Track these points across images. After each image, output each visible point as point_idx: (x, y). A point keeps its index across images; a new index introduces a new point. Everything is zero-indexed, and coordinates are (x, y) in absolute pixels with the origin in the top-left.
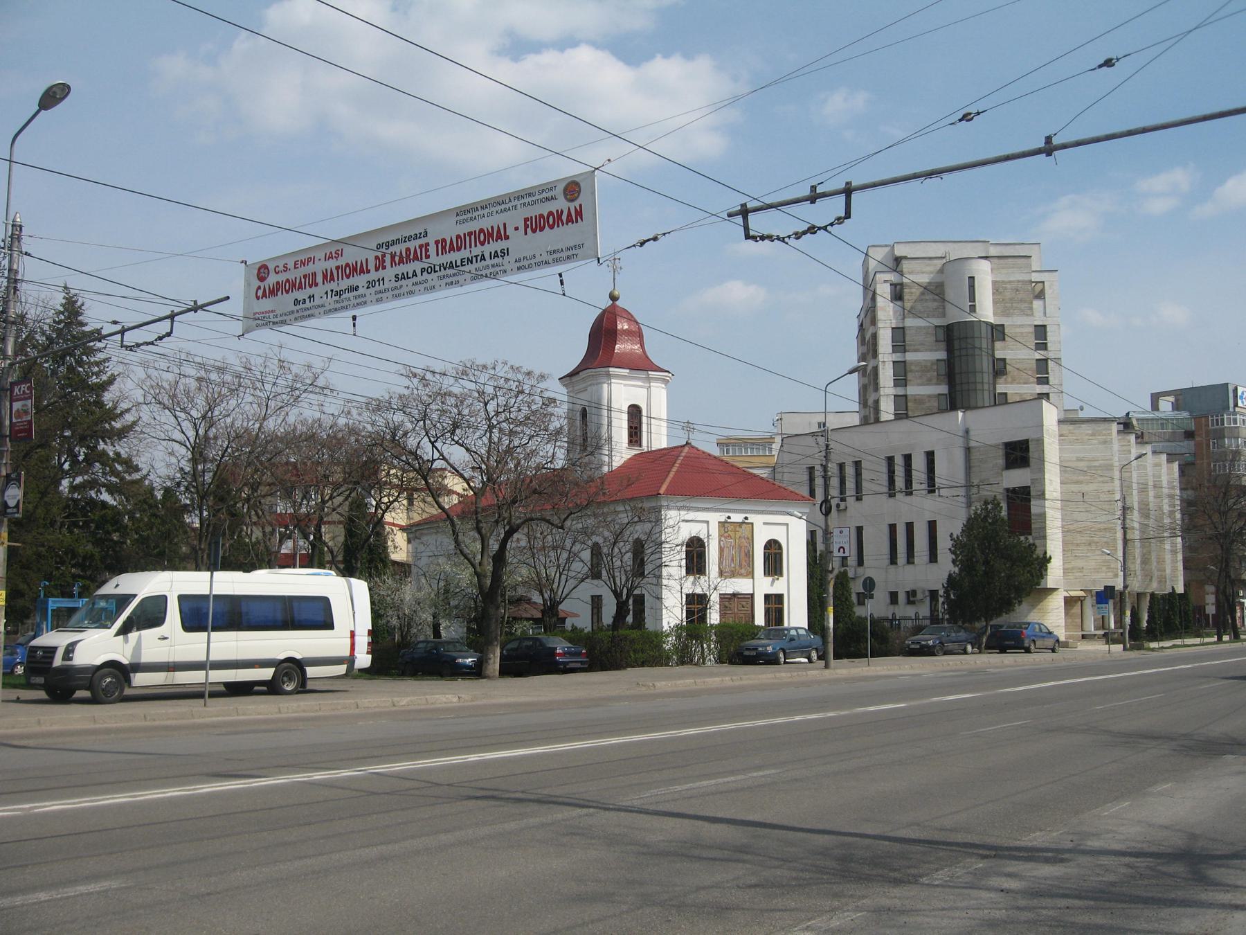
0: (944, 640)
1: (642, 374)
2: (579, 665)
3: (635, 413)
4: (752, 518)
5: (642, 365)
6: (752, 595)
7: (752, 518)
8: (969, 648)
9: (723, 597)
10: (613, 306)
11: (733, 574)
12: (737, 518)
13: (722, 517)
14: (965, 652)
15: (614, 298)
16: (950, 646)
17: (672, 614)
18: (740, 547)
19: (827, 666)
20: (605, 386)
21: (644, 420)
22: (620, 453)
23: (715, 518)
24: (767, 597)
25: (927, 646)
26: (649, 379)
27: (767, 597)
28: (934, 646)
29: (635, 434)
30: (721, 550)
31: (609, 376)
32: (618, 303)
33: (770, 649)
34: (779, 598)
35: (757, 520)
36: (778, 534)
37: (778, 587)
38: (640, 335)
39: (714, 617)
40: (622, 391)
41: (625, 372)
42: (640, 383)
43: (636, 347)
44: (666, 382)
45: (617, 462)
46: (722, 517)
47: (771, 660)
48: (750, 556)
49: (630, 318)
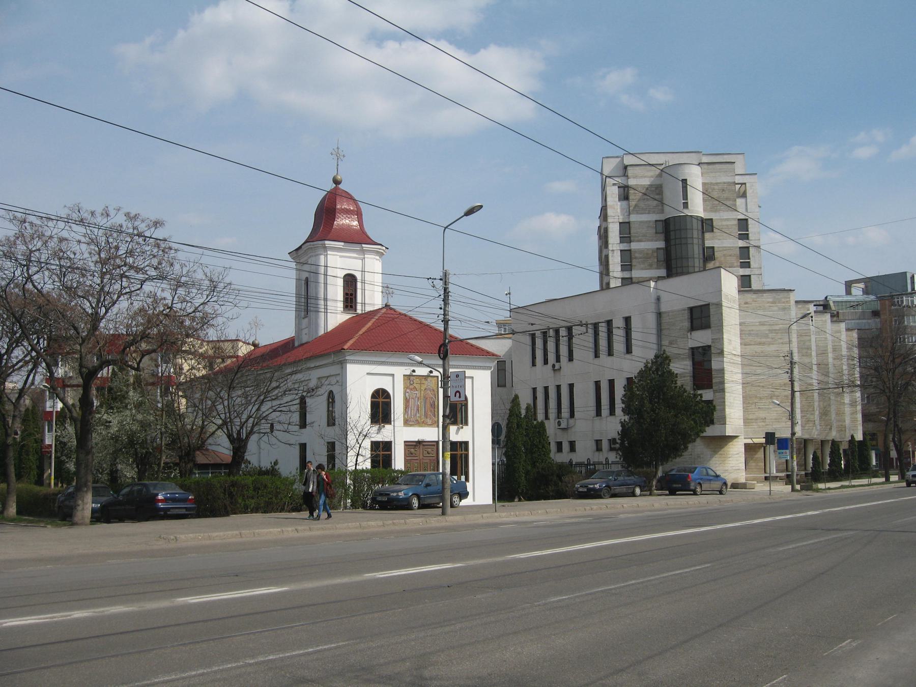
0: (611, 483)
2: (183, 511)
3: (350, 281)
5: (358, 239)
8: (638, 491)
9: (408, 444)
10: (336, 189)
11: (418, 423)
13: (407, 371)
14: (633, 495)
15: (337, 182)
16: (618, 490)
17: (358, 459)
18: (425, 398)
19: (443, 514)
20: (322, 257)
21: (359, 285)
22: (335, 316)
23: (400, 372)
25: (594, 489)
26: (363, 252)
28: (600, 490)
29: (350, 301)
30: (407, 401)
31: (325, 248)
32: (340, 186)
33: (401, 495)
38: (359, 214)
39: (399, 462)
40: (337, 262)
41: (340, 244)
42: (355, 255)
43: (355, 223)
44: (381, 255)
45: (331, 326)
46: (407, 371)
47: (404, 505)
49: (350, 198)
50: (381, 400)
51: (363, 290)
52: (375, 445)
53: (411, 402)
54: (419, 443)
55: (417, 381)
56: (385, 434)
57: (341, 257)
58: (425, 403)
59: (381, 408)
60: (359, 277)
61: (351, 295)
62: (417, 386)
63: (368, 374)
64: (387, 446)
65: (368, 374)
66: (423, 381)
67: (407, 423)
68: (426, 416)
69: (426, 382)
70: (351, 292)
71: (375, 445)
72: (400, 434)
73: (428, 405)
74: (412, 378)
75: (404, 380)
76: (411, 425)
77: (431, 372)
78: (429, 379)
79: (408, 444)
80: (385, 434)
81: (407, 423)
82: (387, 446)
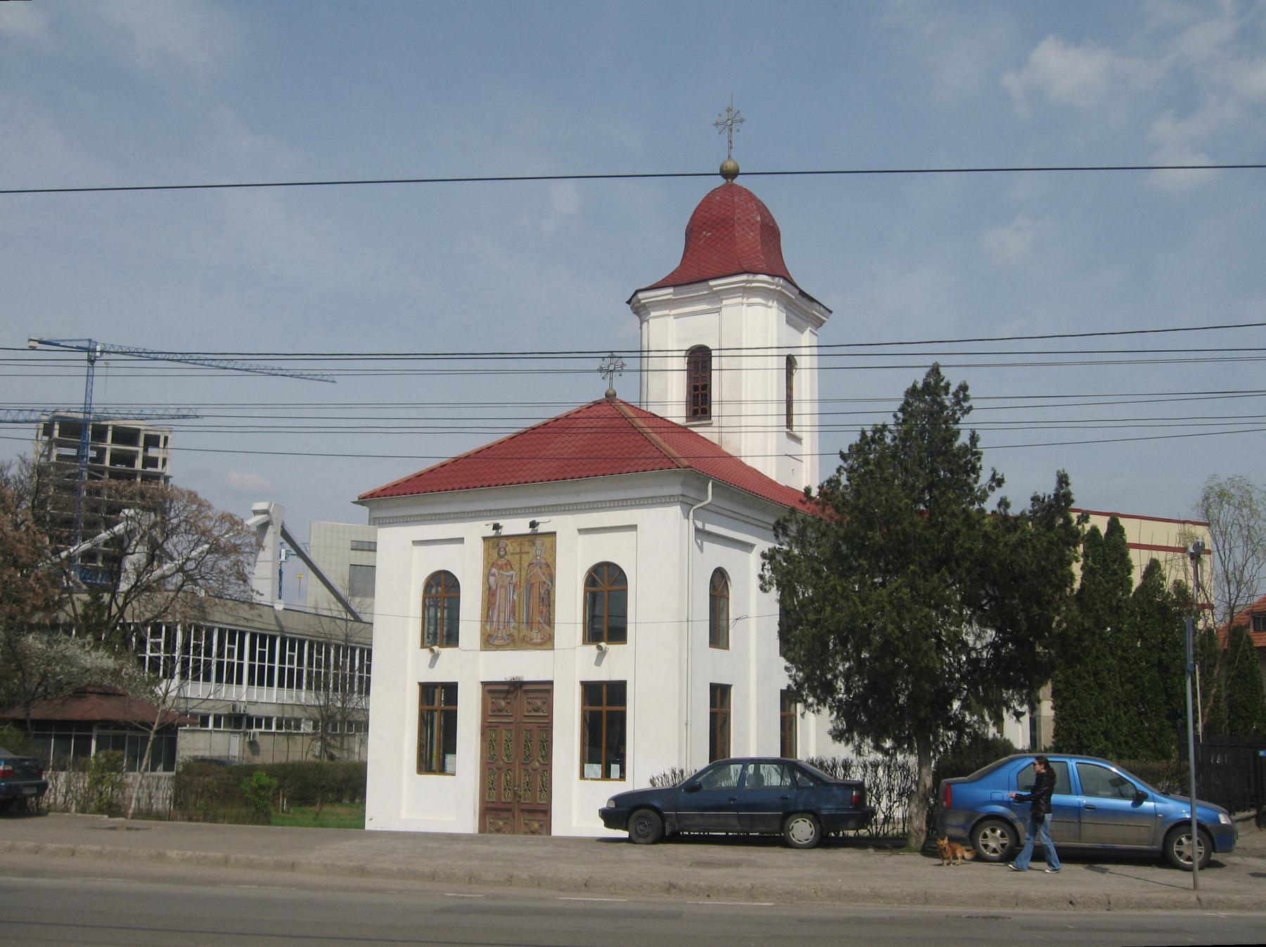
1: (699, 290)
4: (547, 523)
7: (547, 523)
8: (802, 829)
10: (729, 189)
13: (484, 528)
18: (530, 585)
20: (645, 325)
24: (591, 691)
26: (717, 296)
27: (591, 691)
30: (490, 595)
32: (738, 181)
34: (616, 691)
35: (562, 525)
37: (615, 664)
52: (427, 690)
53: (500, 595)
54: (515, 687)
55: (511, 547)
57: (677, 316)
62: (514, 560)
64: (451, 690)
65: (416, 543)
67: (489, 642)
70: (700, 384)
71: (427, 690)
73: (535, 599)
75: (486, 550)
78: (538, 542)
81: (489, 642)
82: (451, 690)
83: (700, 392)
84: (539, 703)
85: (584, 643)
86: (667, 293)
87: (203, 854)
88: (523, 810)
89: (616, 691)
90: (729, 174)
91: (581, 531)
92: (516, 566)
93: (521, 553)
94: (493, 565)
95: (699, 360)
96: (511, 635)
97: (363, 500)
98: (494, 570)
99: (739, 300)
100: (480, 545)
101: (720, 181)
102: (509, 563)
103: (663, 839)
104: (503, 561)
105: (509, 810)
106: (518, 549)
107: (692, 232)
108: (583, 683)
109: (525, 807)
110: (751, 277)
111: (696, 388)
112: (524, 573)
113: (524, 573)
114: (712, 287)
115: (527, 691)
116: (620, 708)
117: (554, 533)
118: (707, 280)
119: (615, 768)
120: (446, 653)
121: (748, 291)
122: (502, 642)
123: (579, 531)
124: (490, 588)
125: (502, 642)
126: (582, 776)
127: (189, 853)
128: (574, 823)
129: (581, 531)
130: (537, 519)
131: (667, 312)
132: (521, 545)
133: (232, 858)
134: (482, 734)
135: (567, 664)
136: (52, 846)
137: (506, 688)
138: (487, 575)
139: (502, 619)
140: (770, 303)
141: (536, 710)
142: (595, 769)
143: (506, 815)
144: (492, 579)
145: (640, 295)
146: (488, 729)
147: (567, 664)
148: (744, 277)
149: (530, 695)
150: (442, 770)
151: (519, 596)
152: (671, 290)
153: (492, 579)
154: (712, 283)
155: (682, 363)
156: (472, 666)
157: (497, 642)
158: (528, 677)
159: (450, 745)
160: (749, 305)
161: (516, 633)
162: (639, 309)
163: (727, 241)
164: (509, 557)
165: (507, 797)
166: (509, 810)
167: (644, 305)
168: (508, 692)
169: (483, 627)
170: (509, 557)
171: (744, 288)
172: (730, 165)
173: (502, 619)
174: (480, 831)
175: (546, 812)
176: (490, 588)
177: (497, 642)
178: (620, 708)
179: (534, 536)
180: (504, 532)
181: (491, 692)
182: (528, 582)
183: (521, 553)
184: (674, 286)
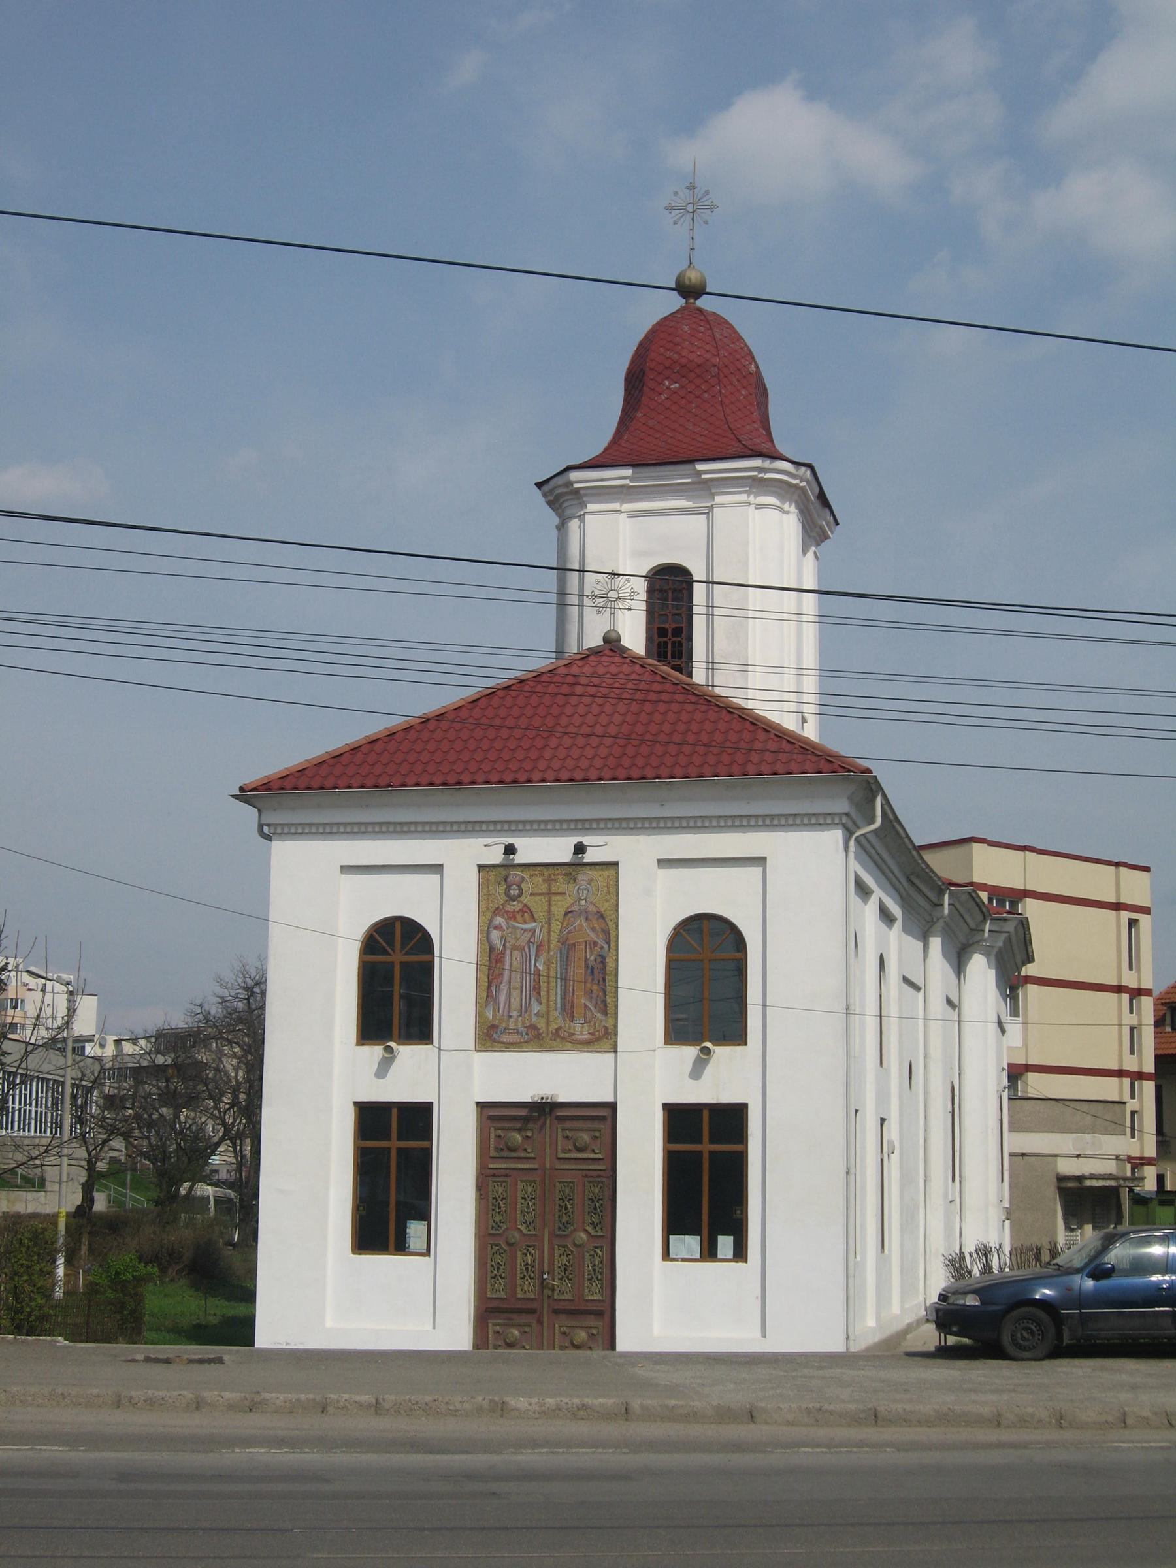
1: (680, 476)
4: (601, 847)
6: (612, 1107)
7: (601, 847)
9: (493, 1115)
11: (536, 1039)
12: (557, 849)
15: (689, 290)
18: (568, 947)
20: (574, 525)
23: (465, 856)
24: (681, 1120)
26: (707, 487)
27: (681, 1120)
32: (704, 303)
34: (730, 1120)
35: (633, 854)
36: (725, 895)
37: (725, 1078)
48: (600, 977)
50: (397, 957)
51: (710, 616)
52: (372, 1119)
53: (512, 960)
54: (542, 1111)
56: (409, 1074)
57: (633, 515)
58: (566, 960)
59: (394, 986)
60: (698, 573)
61: (678, 631)
62: (538, 905)
63: (345, 869)
64: (417, 1119)
65: (345, 869)
66: (560, 885)
67: (490, 1036)
68: (569, 1009)
69: (572, 889)
70: (669, 625)
71: (372, 1119)
72: (458, 1076)
73: (577, 971)
74: (514, 876)
75: (483, 885)
76: (509, 1047)
77: (580, 849)
78: (583, 876)
79: (493, 1115)
80: (409, 1074)
81: (490, 1036)
82: (417, 1119)
83: (670, 639)
84: (585, 1137)
85: (666, 1043)
86: (621, 476)
87: (577, 1401)
88: (556, 1312)
89: (730, 1120)
90: (689, 290)
91: (663, 863)
92: (540, 914)
93: (549, 894)
94: (497, 912)
95: (670, 589)
96: (533, 1027)
97: (247, 795)
98: (499, 920)
99: (744, 497)
100: (474, 876)
101: (675, 302)
102: (526, 910)
103: (1059, 1352)
104: (515, 906)
105: (532, 1311)
106: (544, 888)
107: (637, 380)
108: (666, 1106)
109: (561, 1306)
110: (767, 464)
111: (662, 632)
112: (556, 926)
113: (556, 926)
114: (700, 473)
115: (560, 1119)
116: (424, 1144)
117: (616, 864)
118: (692, 461)
119: (725, 1244)
120: (408, 1054)
121: (758, 484)
122: (515, 1038)
123: (659, 861)
124: (492, 949)
125: (515, 1038)
126: (666, 1255)
127: (550, 1401)
128: (656, 1331)
129: (663, 863)
130: (586, 840)
131: (616, 506)
132: (549, 880)
133: (636, 1404)
134: (479, 1188)
135: (642, 1076)
136: (279, 1398)
137: (523, 1112)
138: (486, 929)
139: (515, 1004)
140: (786, 507)
141: (580, 1150)
142: (691, 1244)
143: (524, 1319)
144: (495, 935)
145: (574, 475)
146: (488, 1180)
147: (642, 1076)
148: (757, 462)
149: (568, 1124)
150: (401, 1247)
151: (548, 964)
152: (628, 472)
153: (495, 935)
154: (700, 467)
155: (641, 586)
156: (458, 1076)
157: (506, 1038)
158: (565, 1096)
159: (418, 1205)
160: (759, 507)
161: (541, 1024)
162: (561, 495)
163: (689, 402)
164: (526, 899)
165: (526, 1290)
166: (532, 1311)
167: (578, 491)
168: (526, 1120)
169: (479, 1015)
170: (526, 899)
171: (753, 478)
172: (693, 276)
173: (515, 1004)
174: (476, 1346)
175: (606, 1313)
176: (492, 949)
177: (506, 1038)
178: (424, 1144)
179: (577, 864)
180: (519, 858)
181: (490, 1118)
182: (563, 941)
183: (549, 894)
184: (633, 466)
